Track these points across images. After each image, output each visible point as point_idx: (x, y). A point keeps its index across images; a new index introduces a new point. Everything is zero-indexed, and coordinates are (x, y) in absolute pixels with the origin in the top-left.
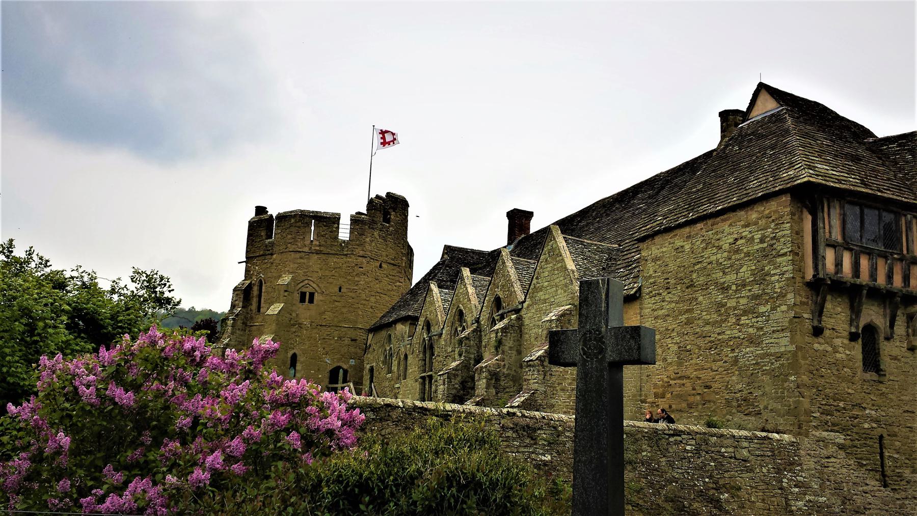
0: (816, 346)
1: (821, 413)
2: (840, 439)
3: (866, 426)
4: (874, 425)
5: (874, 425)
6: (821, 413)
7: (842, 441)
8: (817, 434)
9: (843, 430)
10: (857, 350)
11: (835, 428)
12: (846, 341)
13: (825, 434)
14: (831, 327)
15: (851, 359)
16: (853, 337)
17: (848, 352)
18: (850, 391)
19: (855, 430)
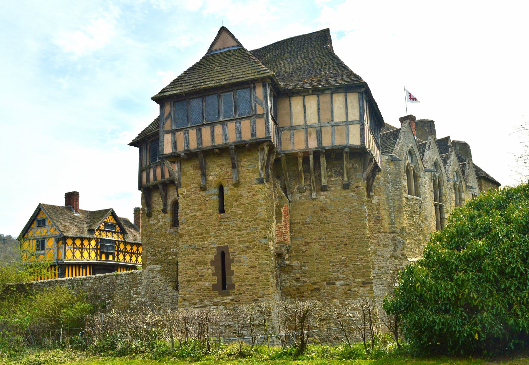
0: (151, 222)
1: (152, 256)
2: (158, 267)
3: (170, 258)
4: (174, 257)
5: (174, 257)
6: (152, 256)
7: (159, 268)
8: (149, 267)
9: (160, 263)
10: (168, 218)
11: (157, 262)
12: (163, 215)
13: (152, 266)
14: (156, 210)
15: (165, 223)
16: (164, 211)
17: (164, 220)
18: (164, 241)
19: (165, 261)
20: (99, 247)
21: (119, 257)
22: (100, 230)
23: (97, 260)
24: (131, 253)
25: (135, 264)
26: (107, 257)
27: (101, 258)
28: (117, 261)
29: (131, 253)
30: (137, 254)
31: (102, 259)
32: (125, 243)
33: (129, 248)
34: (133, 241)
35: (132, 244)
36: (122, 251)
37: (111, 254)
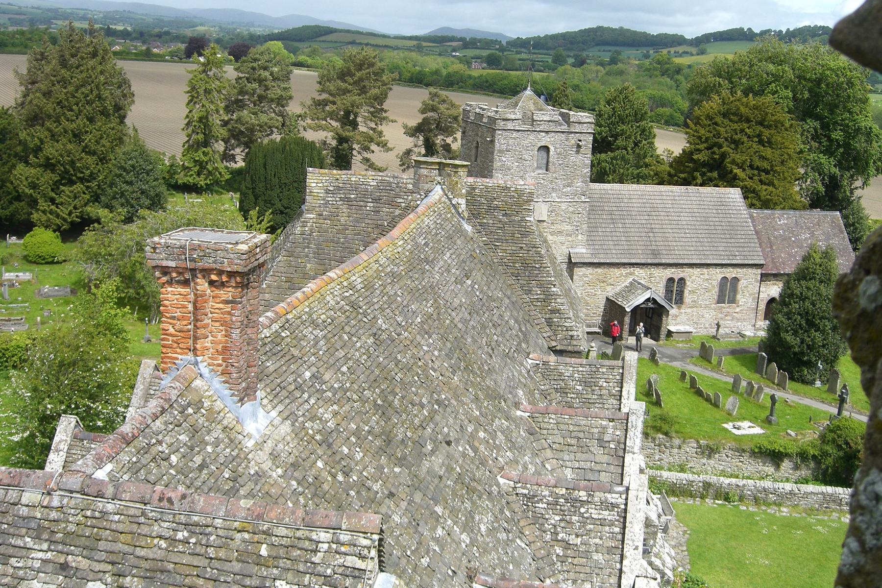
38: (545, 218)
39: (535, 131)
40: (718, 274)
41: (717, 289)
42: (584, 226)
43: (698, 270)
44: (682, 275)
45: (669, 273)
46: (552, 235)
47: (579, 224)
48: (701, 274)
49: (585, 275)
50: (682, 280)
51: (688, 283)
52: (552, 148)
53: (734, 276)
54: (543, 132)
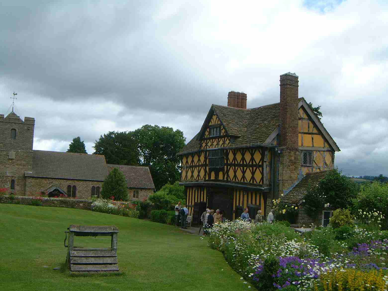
20: (207, 163)
21: (229, 173)
22: (207, 139)
23: (205, 180)
24: (243, 166)
25: (251, 184)
26: (217, 175)
27: (210, 177)
28: (227, 181)
29: (243, 166)
30: (254, 166)
31: (212, 179)
32: (235, 151)
33: (239, 157)
34: (244, 145)
35: (243, 150)
36: (231, 165)
37: (222, 170)
38: (14, 158)
39: (10, 123)
40: (91, 185)
41: (90, 191)
42: (31, 162)
43: (82, 183)
44: (74, 184)
45: (69, 183)
46: (17, 165)
47: (29, 161)
48: (83, 185)
49: (31, 182)
50: (75, 187)
51: (77, 188)
52: (17, 130)
53: (98, 186)
54: (13, 123)
